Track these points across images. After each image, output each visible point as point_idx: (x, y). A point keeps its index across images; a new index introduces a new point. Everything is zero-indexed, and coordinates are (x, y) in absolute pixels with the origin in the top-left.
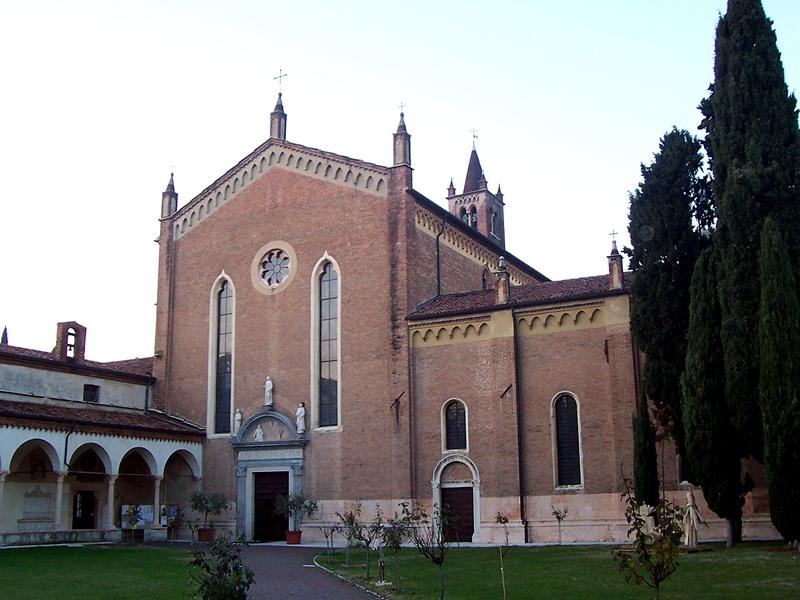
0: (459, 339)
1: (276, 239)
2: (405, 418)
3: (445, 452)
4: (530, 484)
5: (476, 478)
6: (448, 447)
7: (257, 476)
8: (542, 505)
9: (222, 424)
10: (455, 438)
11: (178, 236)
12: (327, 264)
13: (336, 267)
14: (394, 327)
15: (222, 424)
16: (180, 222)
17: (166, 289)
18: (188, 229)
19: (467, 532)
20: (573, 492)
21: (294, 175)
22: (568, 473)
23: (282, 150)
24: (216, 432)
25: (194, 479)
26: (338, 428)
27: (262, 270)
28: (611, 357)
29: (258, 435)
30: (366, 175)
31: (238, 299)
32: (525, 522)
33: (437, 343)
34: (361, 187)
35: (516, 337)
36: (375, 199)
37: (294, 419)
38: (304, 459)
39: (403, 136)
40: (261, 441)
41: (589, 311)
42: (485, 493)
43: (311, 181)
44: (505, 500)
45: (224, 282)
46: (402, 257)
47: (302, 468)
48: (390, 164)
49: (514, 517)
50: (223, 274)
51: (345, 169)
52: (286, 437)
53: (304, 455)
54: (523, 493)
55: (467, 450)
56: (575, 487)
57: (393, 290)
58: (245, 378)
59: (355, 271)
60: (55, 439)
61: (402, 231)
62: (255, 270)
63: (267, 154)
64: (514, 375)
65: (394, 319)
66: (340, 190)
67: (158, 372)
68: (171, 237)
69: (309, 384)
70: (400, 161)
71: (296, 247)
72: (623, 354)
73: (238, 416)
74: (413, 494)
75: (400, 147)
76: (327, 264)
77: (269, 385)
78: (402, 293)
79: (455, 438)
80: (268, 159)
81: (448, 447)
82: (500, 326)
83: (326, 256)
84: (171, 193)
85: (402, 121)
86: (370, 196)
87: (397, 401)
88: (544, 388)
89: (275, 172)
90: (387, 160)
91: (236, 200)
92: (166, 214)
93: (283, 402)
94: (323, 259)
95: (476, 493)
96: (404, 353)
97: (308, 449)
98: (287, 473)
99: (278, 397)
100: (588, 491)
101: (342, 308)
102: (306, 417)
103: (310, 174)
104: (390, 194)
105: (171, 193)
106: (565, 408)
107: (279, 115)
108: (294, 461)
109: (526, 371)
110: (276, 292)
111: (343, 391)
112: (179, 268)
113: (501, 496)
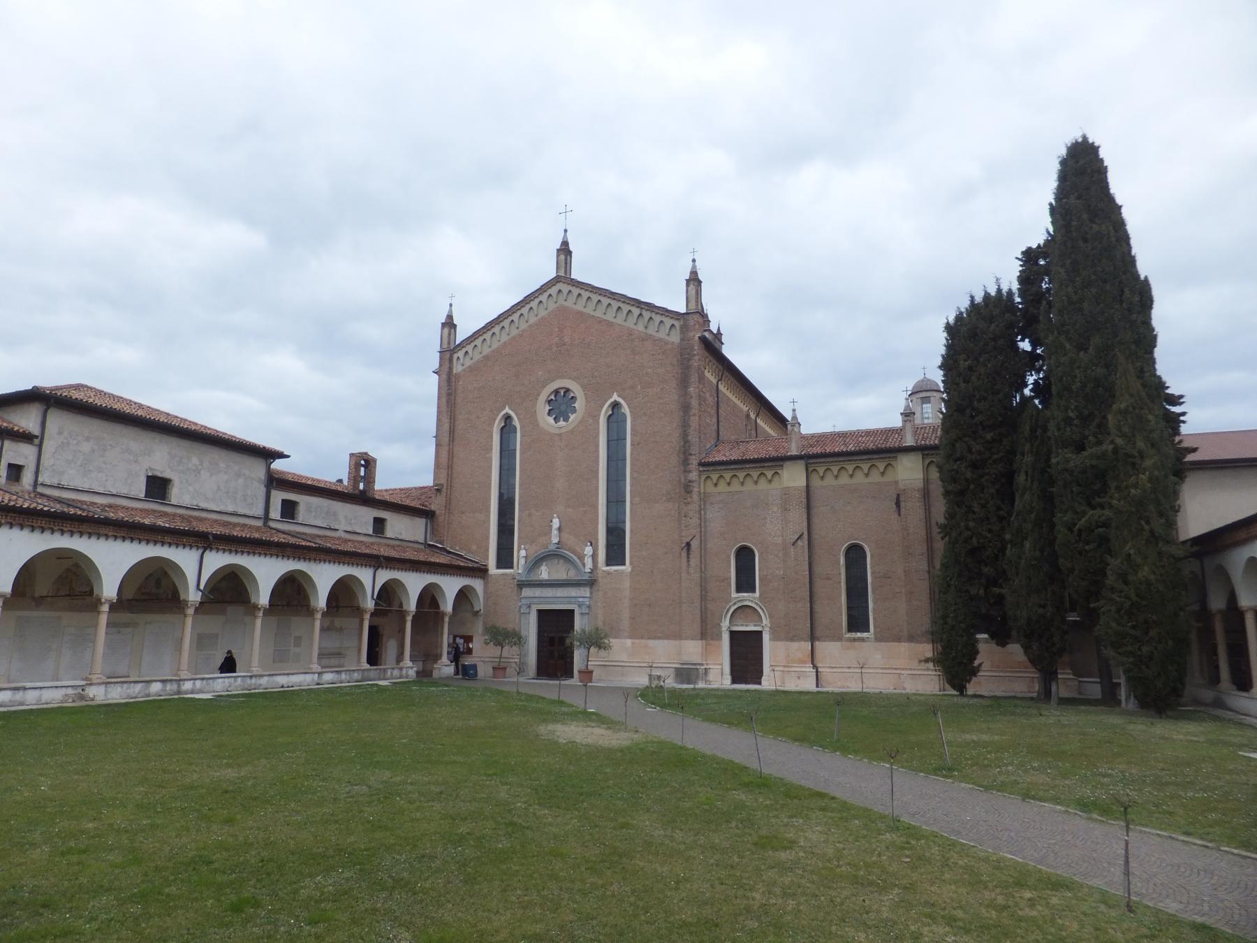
0: (749, 486)
1: (562, 377)
2: (694, 561)
3: (734, 595)
4: (818, 633)
5: (766, 621)
6: (739, 590)
7: (540, 612)
8: (828, 649)
9: (505, 558)
10: (745, 582)
11: (458, 368)
12: (616, 405)
13: (626, 409)
14: (686, 471)
15: (505, 558)
16: (461, 354)
17: (446, 421)
18: (468, 363)
19: (757, 677)
20: (862, 640)
21: (580, 314)
22: (857, 622)
23: (570, 288)
24: (498, 567)
25: (476, 613)
26: (627, 568)
27: (548, 408)
28: (903, 511)
29: (544, 573)
30: (657, 318)
31: (522, 436)
32: (815, 667)
33: (729, 489)
34: (651, 330)
35: (808, 486)
36: (666, 343)
37: (582, 558)
39: (694, 281)
41: (881, 466)
42: (775, 637)
43: (600, 321)
44: (795, 645)
45: (508, 418)
46: (694, 403)
47: (589, 607)
48: (683, 310)
49: (805, 662)
50: (507, 410)
51: (636, 311)
52: (573, 575)
54: (813, 638)
55: (757, 594)
56: (865, 635)
57: (685, 435)
58: (530, 515)
59: (645, 414)
60: (364, 575)
61: (694, 378)
62: (542, 408)
63: (553, 291)
64: (805, 524)
65: (685, 462)
66: (630, 332)
67: (436, 505)
68: (451, 368)
70: (693, 306)
71: (584, 387)
72: (914, 508)
73: (523, 553)
74: (703, 635)
75: (692, 292)
76: (616, 405)
77: (556, 523)
78: (693, 438)
79: (745, 582)
80: (554, 295)
81: (739, 590)
82: (794, 477)
83: (615, 397)
84: (449, 324)
85: (694, 267)
86: (660, 340)
87: (688, 544)
88: (834, 536)
89: (562, 311)
90: (679, 305)
91: (521, 336)
92: (445, 346)
93: (570, 540)
94: (612, 400)
95: (766, 637)
96: (695, 497)
97: (595, 588)
98: (573, 611)
99: (565, 535)
100: (879, 638)
101: (632, 450)
102: (594, 556)
103: (599, 314)
104: (682, 340)
105: (449, 324)
106: (855, 555)
107: (565, 251)
109: (816, 521)
110: (563, 430)
111: (631, 531)
112: (459, 400)
113: (792, 640)
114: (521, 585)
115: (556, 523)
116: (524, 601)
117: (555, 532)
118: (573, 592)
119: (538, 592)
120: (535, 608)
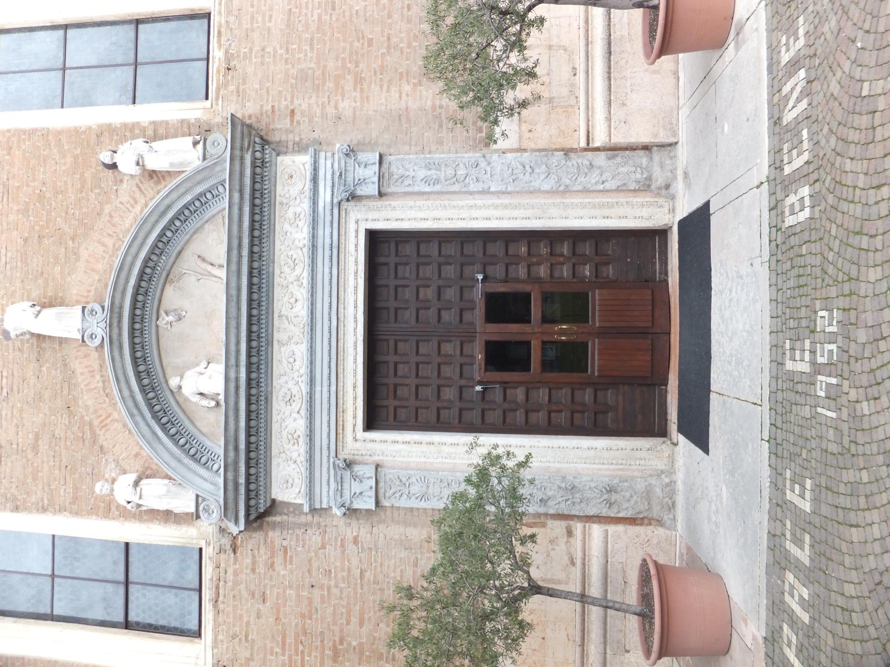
7: (372, 422)
29: (201, 379)
38: (316, 147)
53: (300, 148)
69: (45, 134)
97: (280, 129)
98: (376, 241)
108: (325, 195)
114: (255, 508)
115: (20, 318)
116: (326, 497)
118: (291, 237)
119: (287, 421)
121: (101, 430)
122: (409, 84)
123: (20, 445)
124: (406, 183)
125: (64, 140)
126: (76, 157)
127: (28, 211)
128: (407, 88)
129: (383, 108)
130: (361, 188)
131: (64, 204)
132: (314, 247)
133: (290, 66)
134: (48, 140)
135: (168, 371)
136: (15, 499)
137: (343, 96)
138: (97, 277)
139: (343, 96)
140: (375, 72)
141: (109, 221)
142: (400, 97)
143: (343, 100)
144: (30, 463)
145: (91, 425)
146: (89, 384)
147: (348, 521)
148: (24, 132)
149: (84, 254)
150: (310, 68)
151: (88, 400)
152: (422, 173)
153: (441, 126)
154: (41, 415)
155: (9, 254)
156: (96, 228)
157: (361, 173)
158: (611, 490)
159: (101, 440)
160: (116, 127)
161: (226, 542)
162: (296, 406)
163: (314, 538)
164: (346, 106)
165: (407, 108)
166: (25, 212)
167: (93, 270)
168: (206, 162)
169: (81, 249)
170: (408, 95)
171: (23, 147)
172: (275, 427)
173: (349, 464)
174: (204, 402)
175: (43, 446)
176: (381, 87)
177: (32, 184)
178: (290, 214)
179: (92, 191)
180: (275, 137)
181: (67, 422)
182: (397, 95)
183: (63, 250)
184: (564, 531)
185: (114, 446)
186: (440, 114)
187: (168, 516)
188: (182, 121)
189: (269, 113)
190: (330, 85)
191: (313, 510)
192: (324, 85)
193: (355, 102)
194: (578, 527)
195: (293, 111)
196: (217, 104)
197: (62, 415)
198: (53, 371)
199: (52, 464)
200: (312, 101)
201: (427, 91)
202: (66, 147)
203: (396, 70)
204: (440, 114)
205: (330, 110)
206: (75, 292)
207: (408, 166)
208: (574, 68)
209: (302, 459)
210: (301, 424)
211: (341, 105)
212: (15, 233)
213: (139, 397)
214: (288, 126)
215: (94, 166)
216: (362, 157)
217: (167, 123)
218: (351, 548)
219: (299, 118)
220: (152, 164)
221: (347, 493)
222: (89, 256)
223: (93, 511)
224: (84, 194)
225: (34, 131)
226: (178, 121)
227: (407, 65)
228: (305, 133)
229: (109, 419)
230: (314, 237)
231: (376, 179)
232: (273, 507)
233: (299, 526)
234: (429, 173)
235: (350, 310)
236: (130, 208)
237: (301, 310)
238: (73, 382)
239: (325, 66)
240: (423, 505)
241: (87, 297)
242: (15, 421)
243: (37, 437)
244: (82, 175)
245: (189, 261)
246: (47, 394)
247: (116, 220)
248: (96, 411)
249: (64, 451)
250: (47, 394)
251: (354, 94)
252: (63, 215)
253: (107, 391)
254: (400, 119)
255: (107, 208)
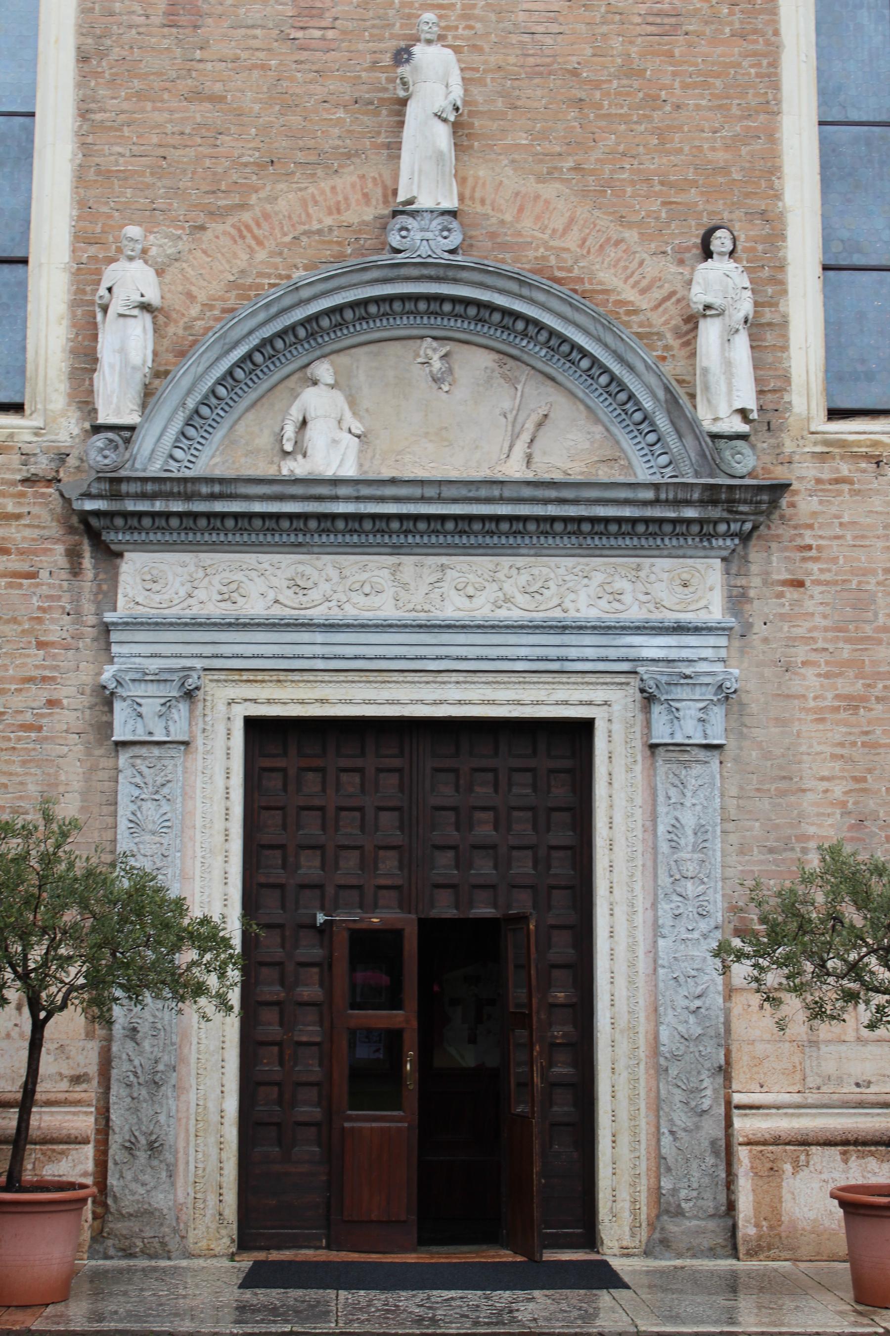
7: (258, 730)
29: (330, 429)
40: (350, 471)
53: (737, 600)
69: (770, 107)
93: (543, 222)
97: (770, 562)
98: (578, 734)
108: (652, 647)
116: (129, 652)
117: (425, 137)
119: (261, 582)
120: (228, 709)
121: (233, 226)
122: (845, 793)
123: (201, 66)
124: (673, 792)
125: (758, 145)
126: (724, 170)
127: (628, 77)
128: (838, 790)
129: (803, 749)
130: (665, 713)
131: (641, 149)
132: (564, 629)
133: (881, 577)
134: (757, 112)
135: (343, 359)
136: (102, 54)
137: (827, 676)
138: (508, 217)
139: (827, 676)
140: (866, 733)
141: (608, 240)
142: (822, 779)
143: (819, 675)
144: (168, 85)
145: (243, 206)
146: (316, 202)
147: (88, 690)
148: (775, 64)
149: (549, 190)
150: (876, 615)
151: (287, 201)
152: (689, 820)
153: (771, 851)
154: (257, 107)
155: (549, 40)
156: (596, 213)
157: (690, 711)
158: (154, 1148)
159: (216, 227)
160: (779, 249)
161: (42, 466)
162: (287, 597)
163: (56, 629)
164: (809, 681)
165: (804, 791)
166: (630, 72)
167: (521, 210)
168: (708, 440)
169: (558, 185)
170: (826, 791)
171: (745, 64)
172: (250, 559)
173: (189, 695)
174: (290, 431)
175: (200, 112)
176: (841, 745)
177: (677, 85)
178: (620, 584)
179: (664, 204)
180: (755, 554)
181: (244, 159)
182: (826, 773)
183: (558, 149)
184: (81, 1071)
185: (205, 252)
186: (792, 849)
187: (85, 359)
188: (787, 379)
189: (799, 542)
190: (846, 651)
191: (106, 629)
192: (848, 640)
193: (815, 698)
194: (90, 1091)
195: (800, 584)
196: (815, 444)
197: (257, 149)
198: (336, 131)
199: (169, 128)
200: (818, 621)
201: (831, 826)
202: (744, 150)
203: (870, 771)
204: (792, 849)
205: (801, 653)
206: (481, 173)
207: (702, 794)
208: (870, 1082)
209: (196, 611)
210: (255, 606)
211: (810, 672)
212: (589, 52)
213: (299, 314)
214: (776, 577)
215: (710, 207)
216: (717, 714)
217: (785, 348)
218: (38, 695)
219: (788, 595)
220: (710, 333)
221: (137, 690)
222: (547, 202)
223: (85, 209)
224: (658, 188)
225: (776, 85)
226: (787, 370)
227: (879, 790)
228: (763, 608)
229: (253, 243)
230: (580, 629)
231: (679, 739)
232: (109, 555)
233: (76, 600)
234: (690, 832)
235: (453, 693)
236: (631, 281)
237: (453, 608)
238: (320, 172)
239: (879, 642)
240: (123, 824)
241: (472, 198)
242: (244, 55)
243: (216, 99)
244: (694, 183)
245: (538, 397)
246: (295, 120)
247: (612, 253)
248: (266, 216)
249: (191, 152)
250: (295, 120)
251: (830, 695)
252: (621, 148)
253: (304, 239)
254: (786, 781)
255: (631, 236)
